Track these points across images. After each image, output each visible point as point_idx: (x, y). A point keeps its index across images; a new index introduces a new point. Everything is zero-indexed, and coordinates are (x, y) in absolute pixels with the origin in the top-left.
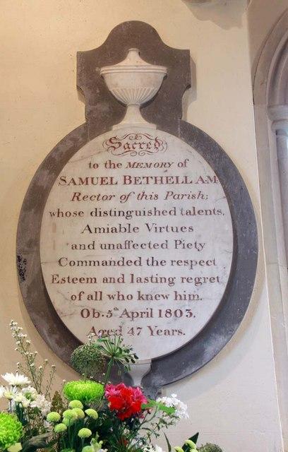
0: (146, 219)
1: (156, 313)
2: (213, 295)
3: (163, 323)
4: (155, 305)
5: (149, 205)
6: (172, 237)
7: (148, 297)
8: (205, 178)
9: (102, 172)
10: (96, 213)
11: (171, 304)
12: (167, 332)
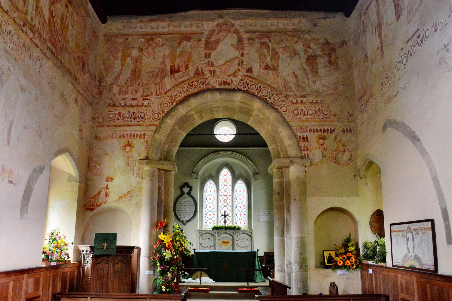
2: (192, 214)
5: (186, 204)
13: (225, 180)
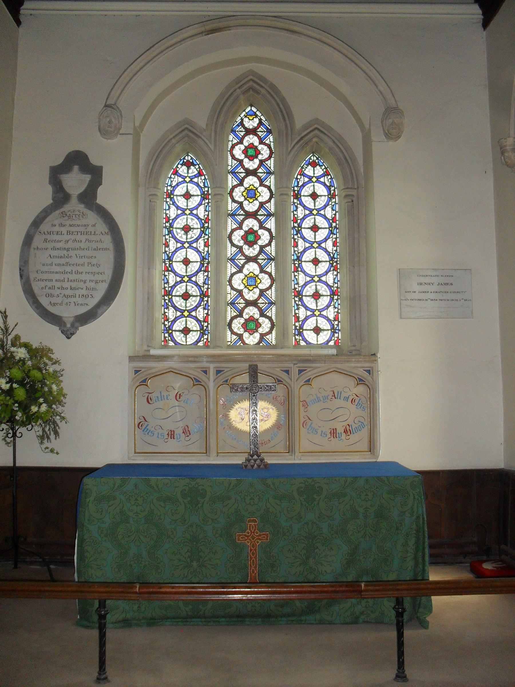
0: (76, 252)
1: (77, 296)
2: (102, 289)
3: (80, 301)
4: (77, 292)
5: (78, 245)
6: (87, 260)
7: (75, 289)
8: (103, 233)
9: (56, 229)
10: (54, 249)
11: (84, 292)
12: (82, 305)
13: (251, 152)
